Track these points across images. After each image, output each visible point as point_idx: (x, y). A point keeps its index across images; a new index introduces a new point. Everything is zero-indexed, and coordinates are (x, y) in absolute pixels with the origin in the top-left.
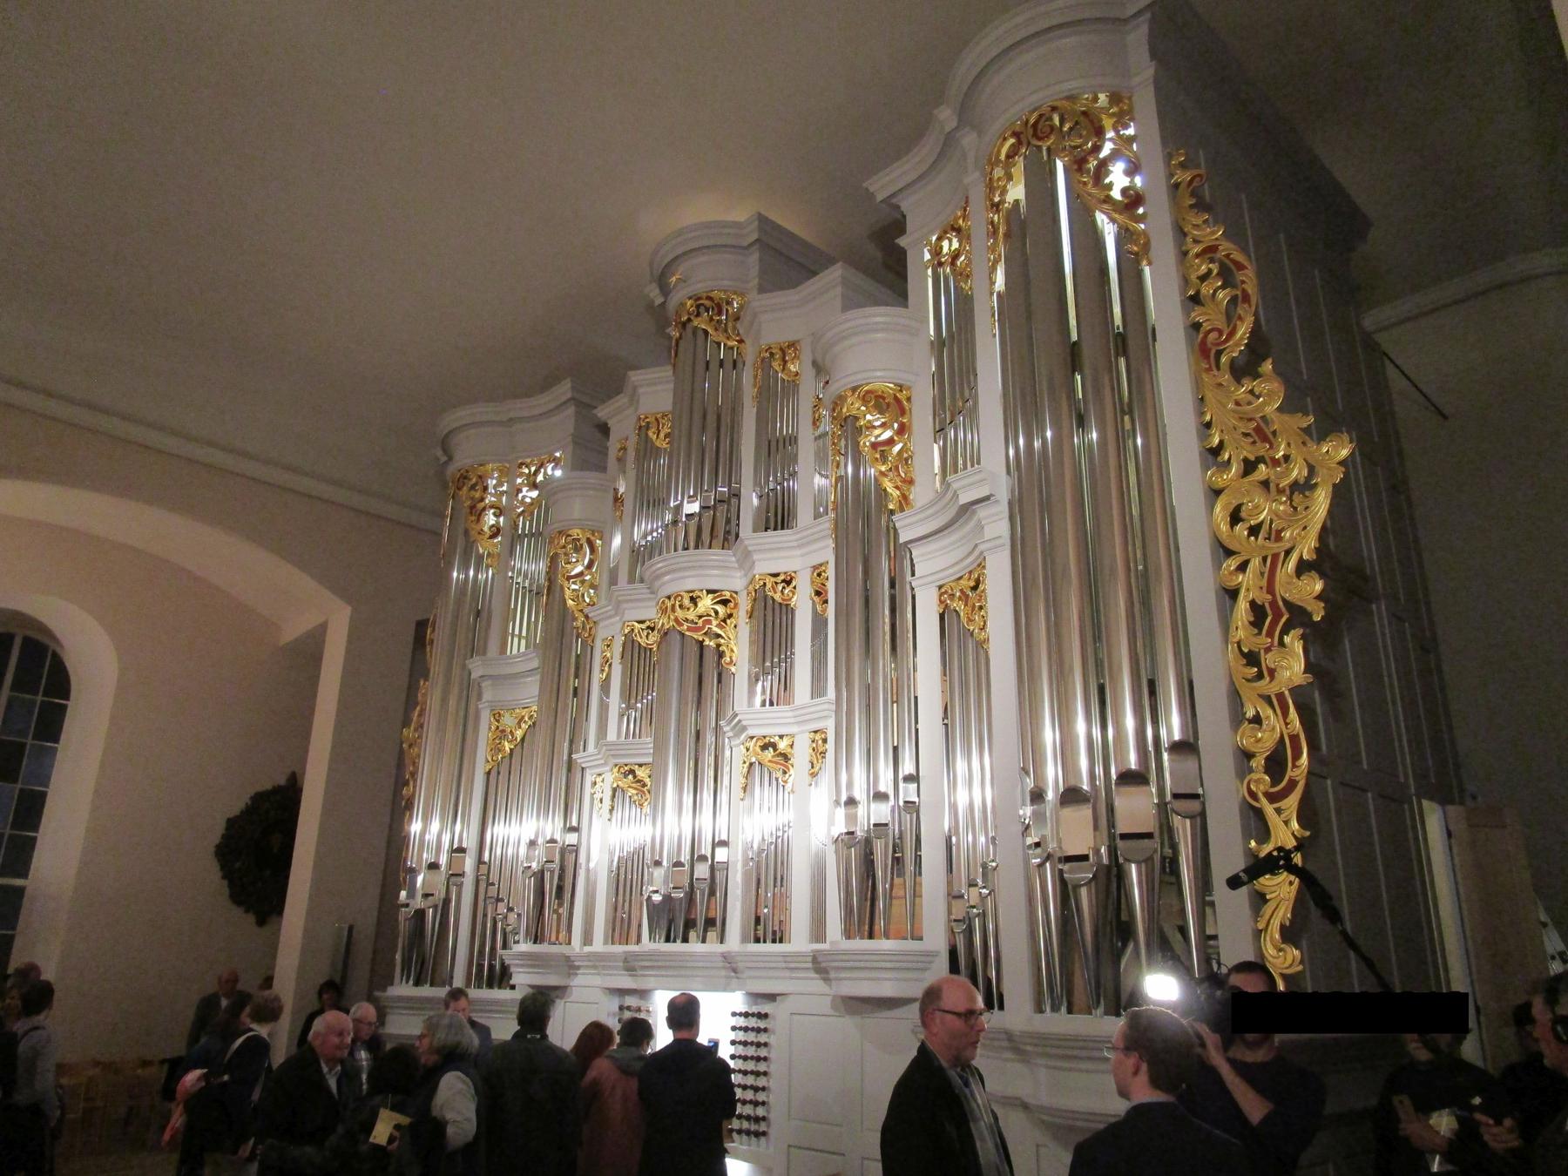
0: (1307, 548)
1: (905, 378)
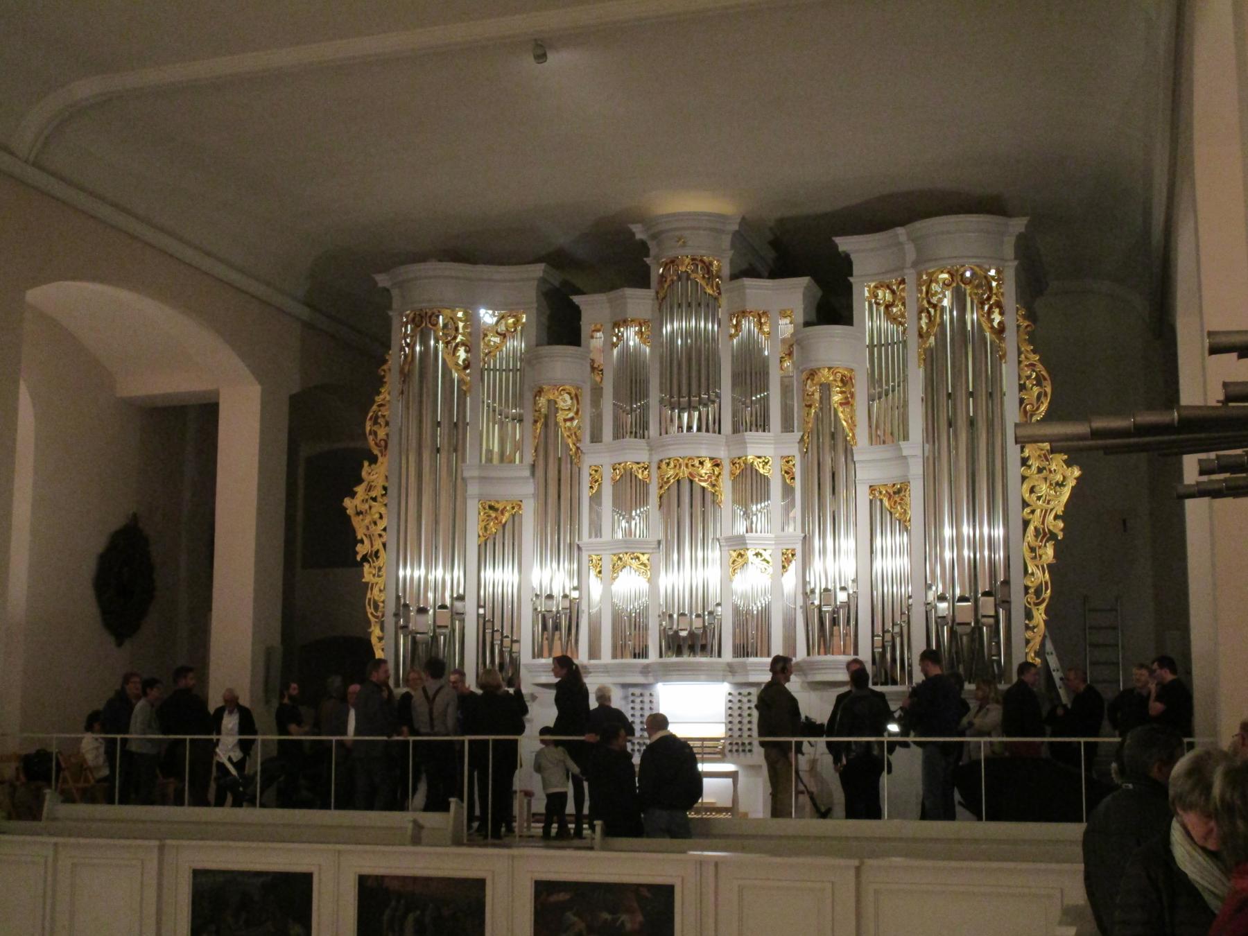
0: (1060, 510)
1: (853, 366)
